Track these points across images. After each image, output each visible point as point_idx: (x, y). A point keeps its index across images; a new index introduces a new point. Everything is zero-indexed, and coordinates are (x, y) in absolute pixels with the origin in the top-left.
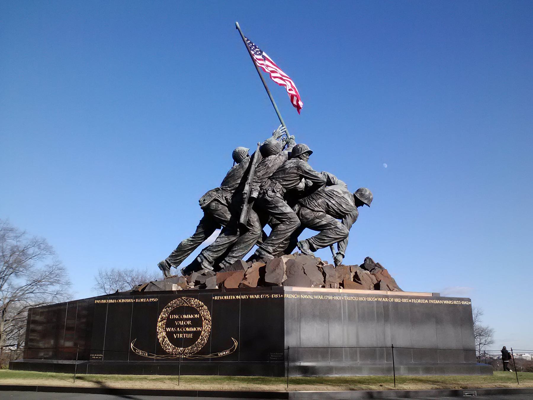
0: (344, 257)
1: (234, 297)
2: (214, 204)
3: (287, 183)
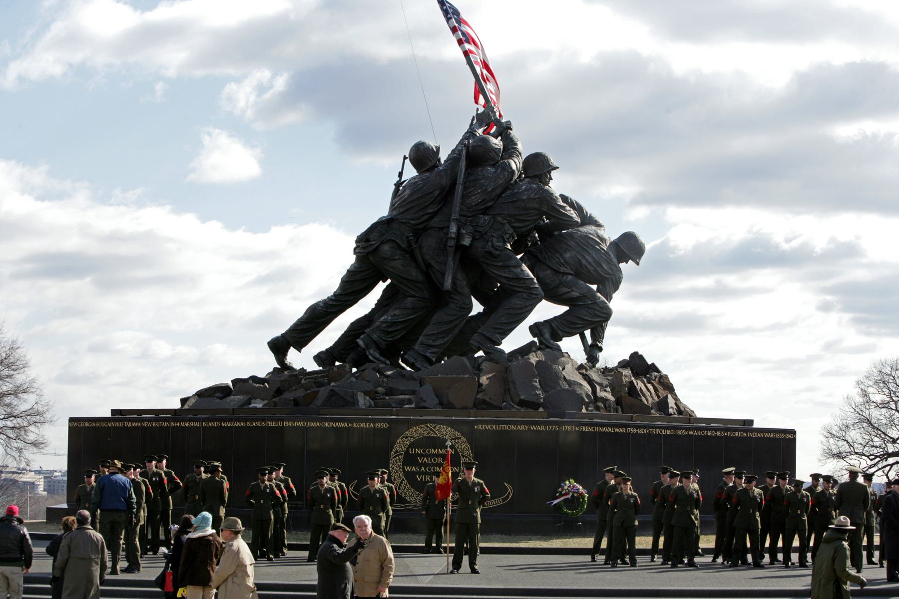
0: (601, 349)
1: (507, 428)
2: (386, 247)
3: (521, 225)
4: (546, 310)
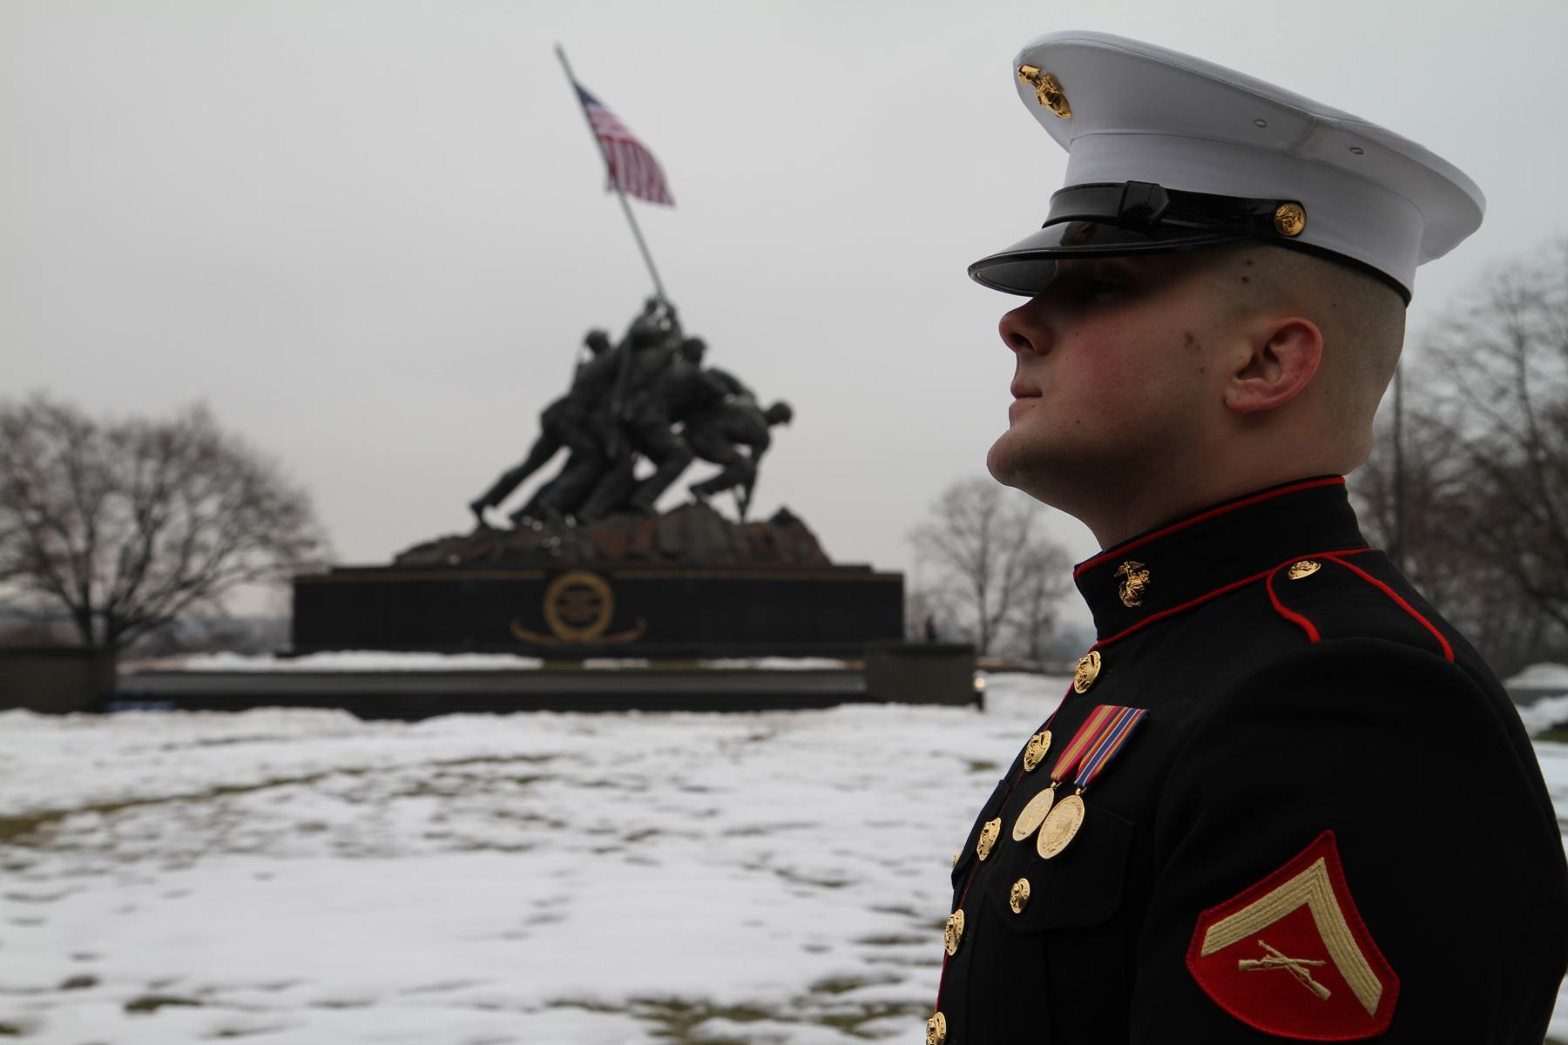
4: (701, 471)
